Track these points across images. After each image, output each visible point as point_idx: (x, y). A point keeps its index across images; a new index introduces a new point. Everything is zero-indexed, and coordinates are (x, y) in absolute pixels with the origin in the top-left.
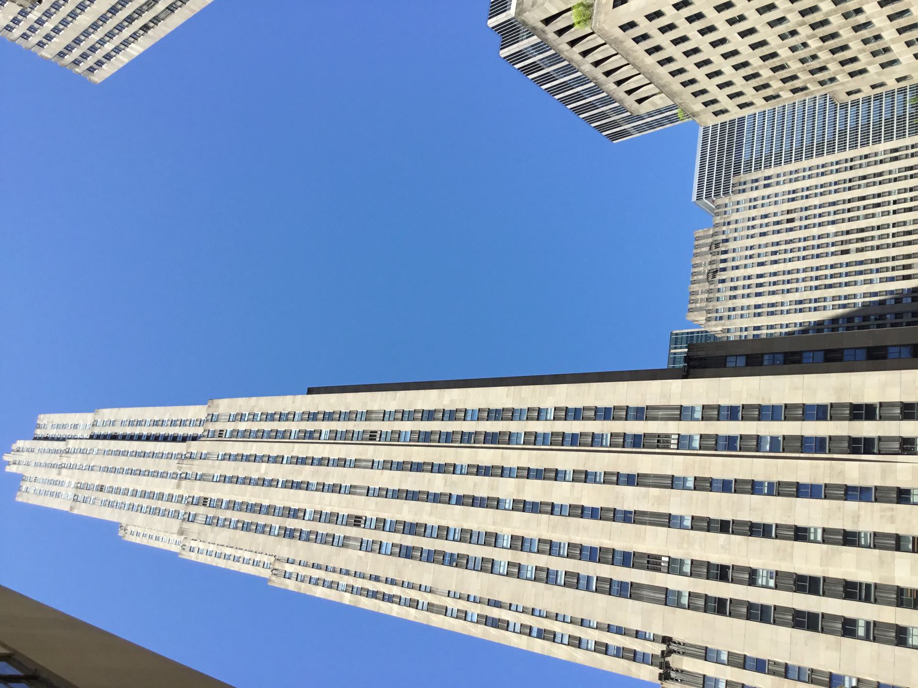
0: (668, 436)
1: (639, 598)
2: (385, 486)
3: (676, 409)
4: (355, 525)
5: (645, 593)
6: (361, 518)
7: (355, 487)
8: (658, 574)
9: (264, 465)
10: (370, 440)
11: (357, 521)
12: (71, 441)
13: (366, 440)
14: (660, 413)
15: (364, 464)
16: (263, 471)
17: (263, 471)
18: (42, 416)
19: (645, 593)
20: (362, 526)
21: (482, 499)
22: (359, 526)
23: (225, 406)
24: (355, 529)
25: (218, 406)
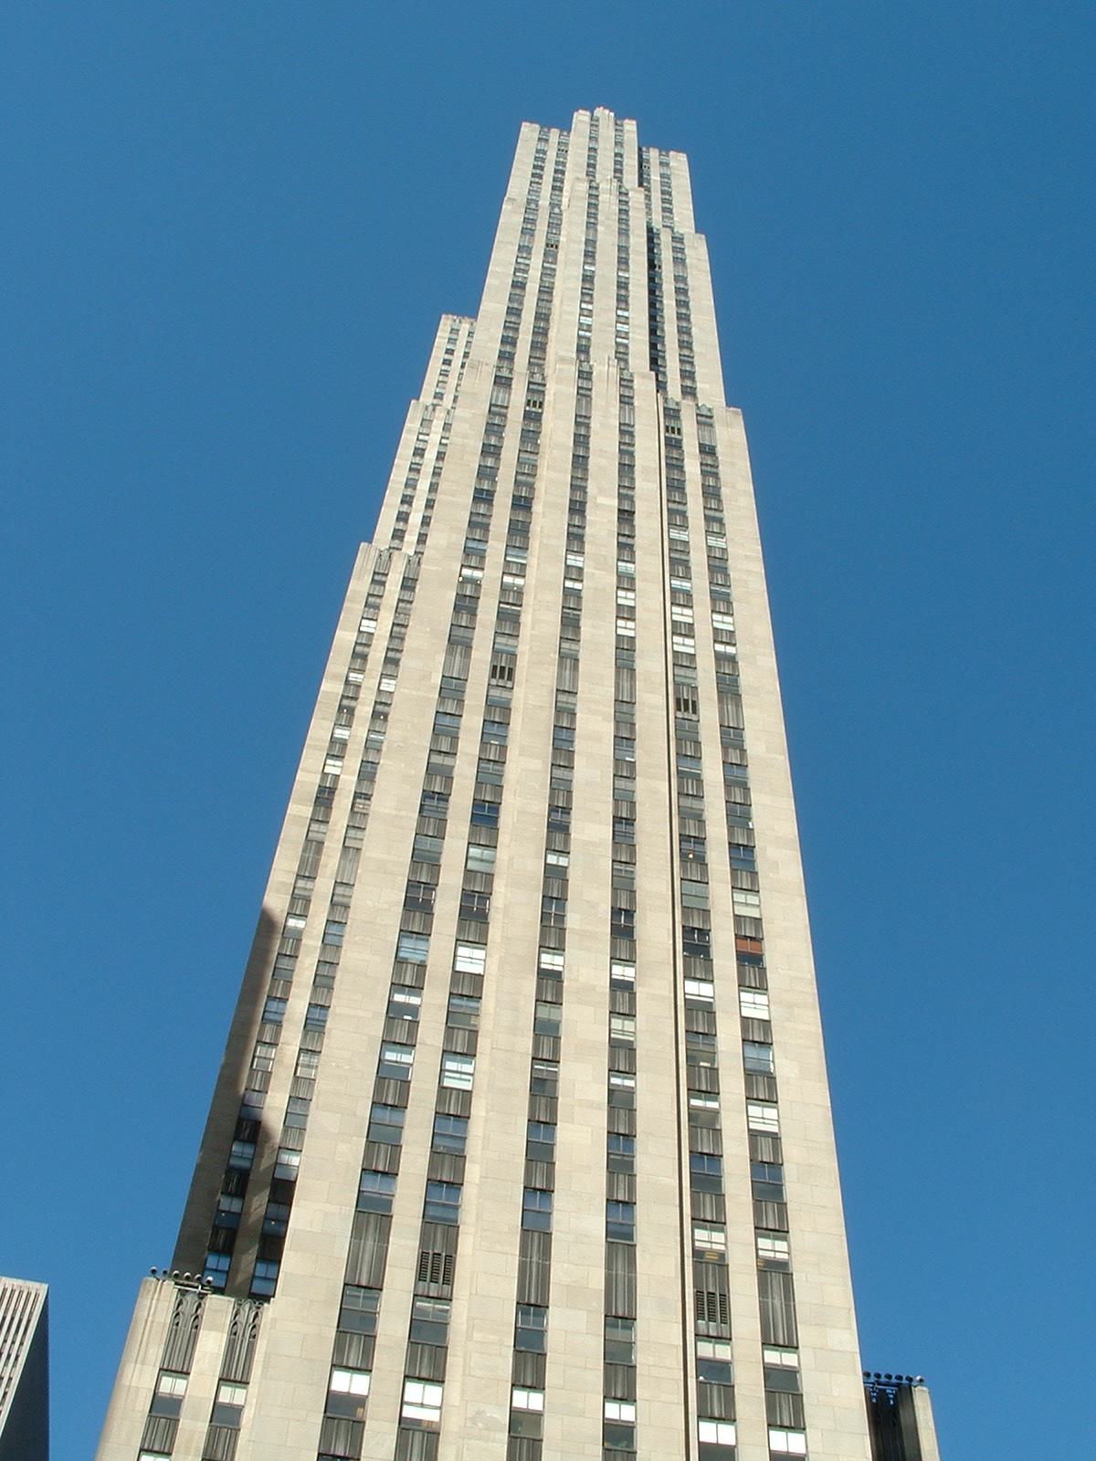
0: (725, 1317)
1: (358, 1230)
2: (579, 725)
4: (495, 668)
5: (370, 1243)
6: (510, 677)
7: (575, 667)
9: (615, 502)
10: (678, 701)
11: (503, 671)
12: (641, 197)
13: (676, 691)
14: (777, 1302)
15: (626, 685)
16: (601, 500)
17: (601, 500)
18: (683, 157)
19: (370, 1243)
20: (494, 682)
21: (561, 918)
22: (493, 675)
23: (732, 436)
25: (728, 425)
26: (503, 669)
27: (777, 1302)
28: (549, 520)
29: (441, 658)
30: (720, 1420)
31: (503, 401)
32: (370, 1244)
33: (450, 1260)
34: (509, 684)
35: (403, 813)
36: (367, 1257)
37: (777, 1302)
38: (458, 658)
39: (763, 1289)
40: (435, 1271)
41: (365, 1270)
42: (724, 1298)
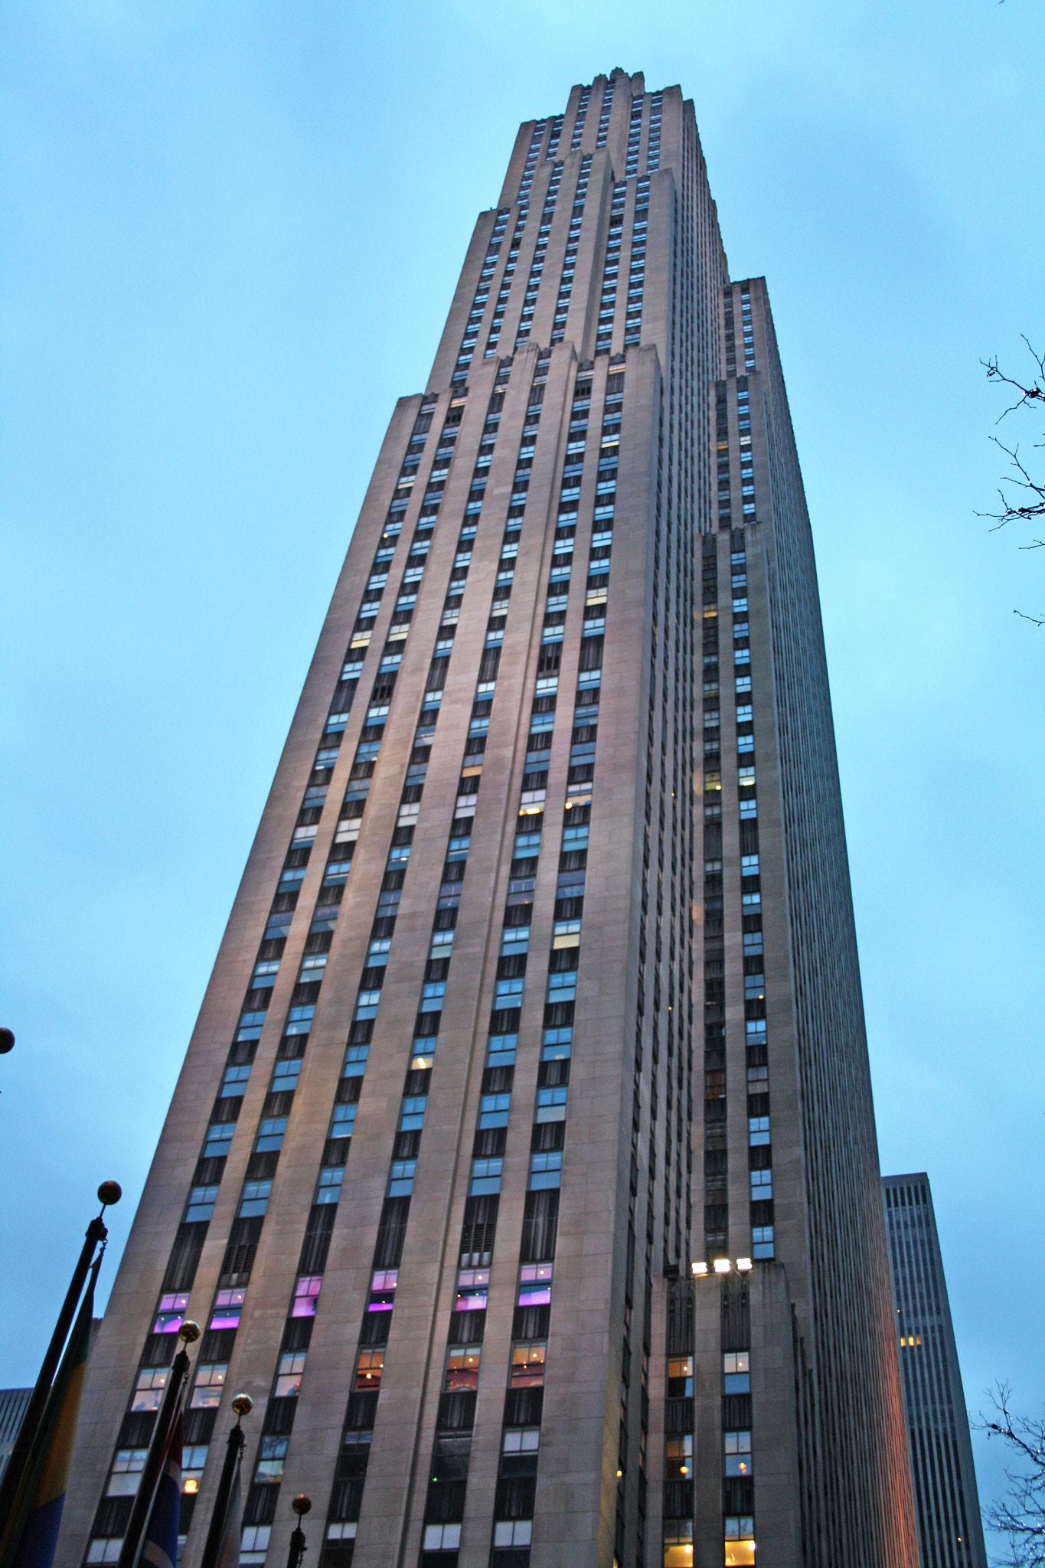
0: (489, 1246)
4: (375, 691)
5: (188, 1249)
14: (541, 1220)
15: (490, 664)
19: (188, 1249)
26: (383, 689)
32: (187, 1252)
36: (183, 1265)
37: (541, 1220)
39: (529, 1212)
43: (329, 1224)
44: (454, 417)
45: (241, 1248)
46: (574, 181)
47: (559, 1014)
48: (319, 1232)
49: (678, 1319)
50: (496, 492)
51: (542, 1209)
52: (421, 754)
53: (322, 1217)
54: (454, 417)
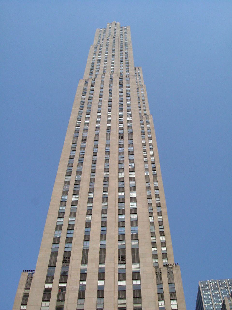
0: (125, 260)
3: (138, 261)
4: (83, 139)
5: (54, 258)
8: (62, 262)
14: (136, 254)
15: (108, 136)
19: (54, 258)
24: (81, 140)
27: (136, 254)
28: (94, 108)
29: (72, 140)
30: (123, 280)
31: (86, 86)
32: (53, 258)
33: (69, 258)
34: (85, 142)
35: (63, 172)
36: (53, 261)
38: (75, 139)
40: (66, 261)
41: (52, 263)
42: (124, 255)
43: (87, 253)
44: (93, 85)
45: (67, 258)
46: (112, 41)
47: (134, 211)
48: (85, 255)
49: (158, 277)
50: (105, 101)
51: (135, 252)
52: (95, 154)
53: (86, 251)
54: (93, 85)
